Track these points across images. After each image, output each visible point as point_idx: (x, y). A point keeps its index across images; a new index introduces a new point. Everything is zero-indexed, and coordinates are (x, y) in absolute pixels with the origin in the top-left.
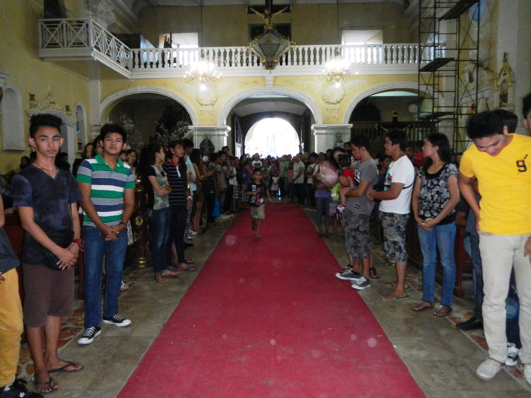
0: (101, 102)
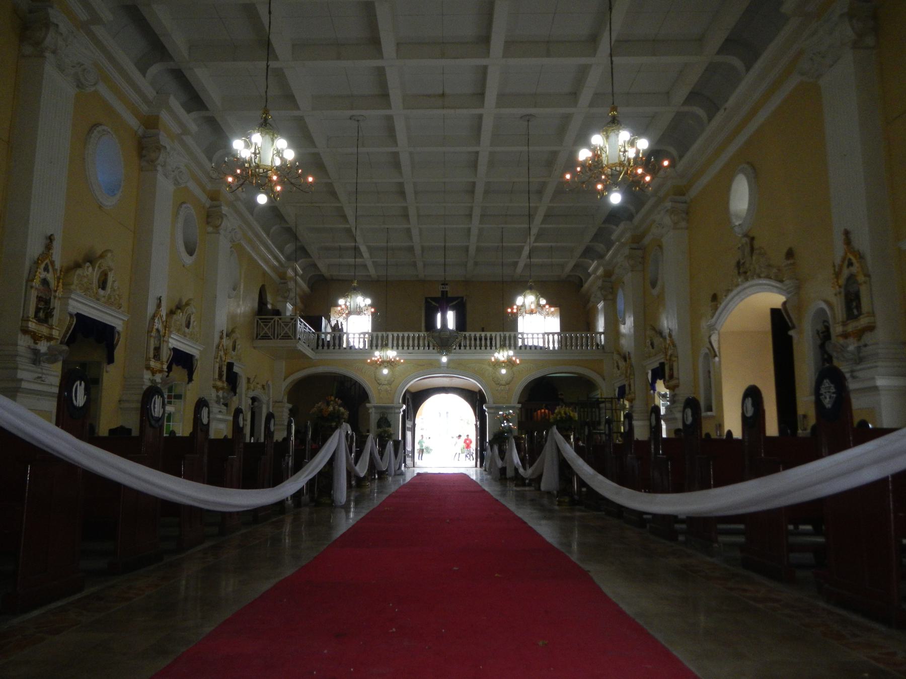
0: (285, 380)
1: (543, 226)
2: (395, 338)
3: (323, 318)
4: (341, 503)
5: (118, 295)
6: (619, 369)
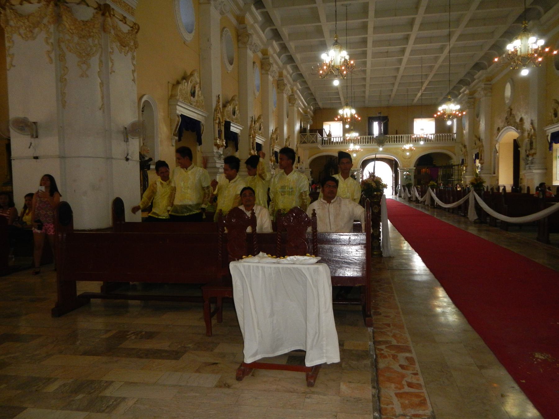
0: (309, 159)
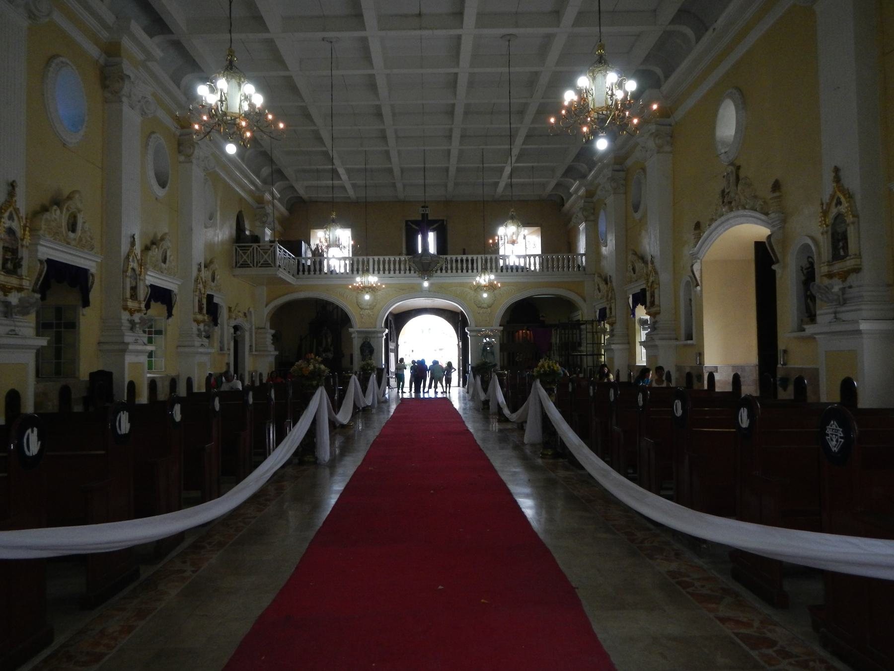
0: (266, 305)
1: (524, 147)
2: (376, 262)
3: (303, 242)
4: (325, 461)
5: (90, 236)
6: (600, 291)
